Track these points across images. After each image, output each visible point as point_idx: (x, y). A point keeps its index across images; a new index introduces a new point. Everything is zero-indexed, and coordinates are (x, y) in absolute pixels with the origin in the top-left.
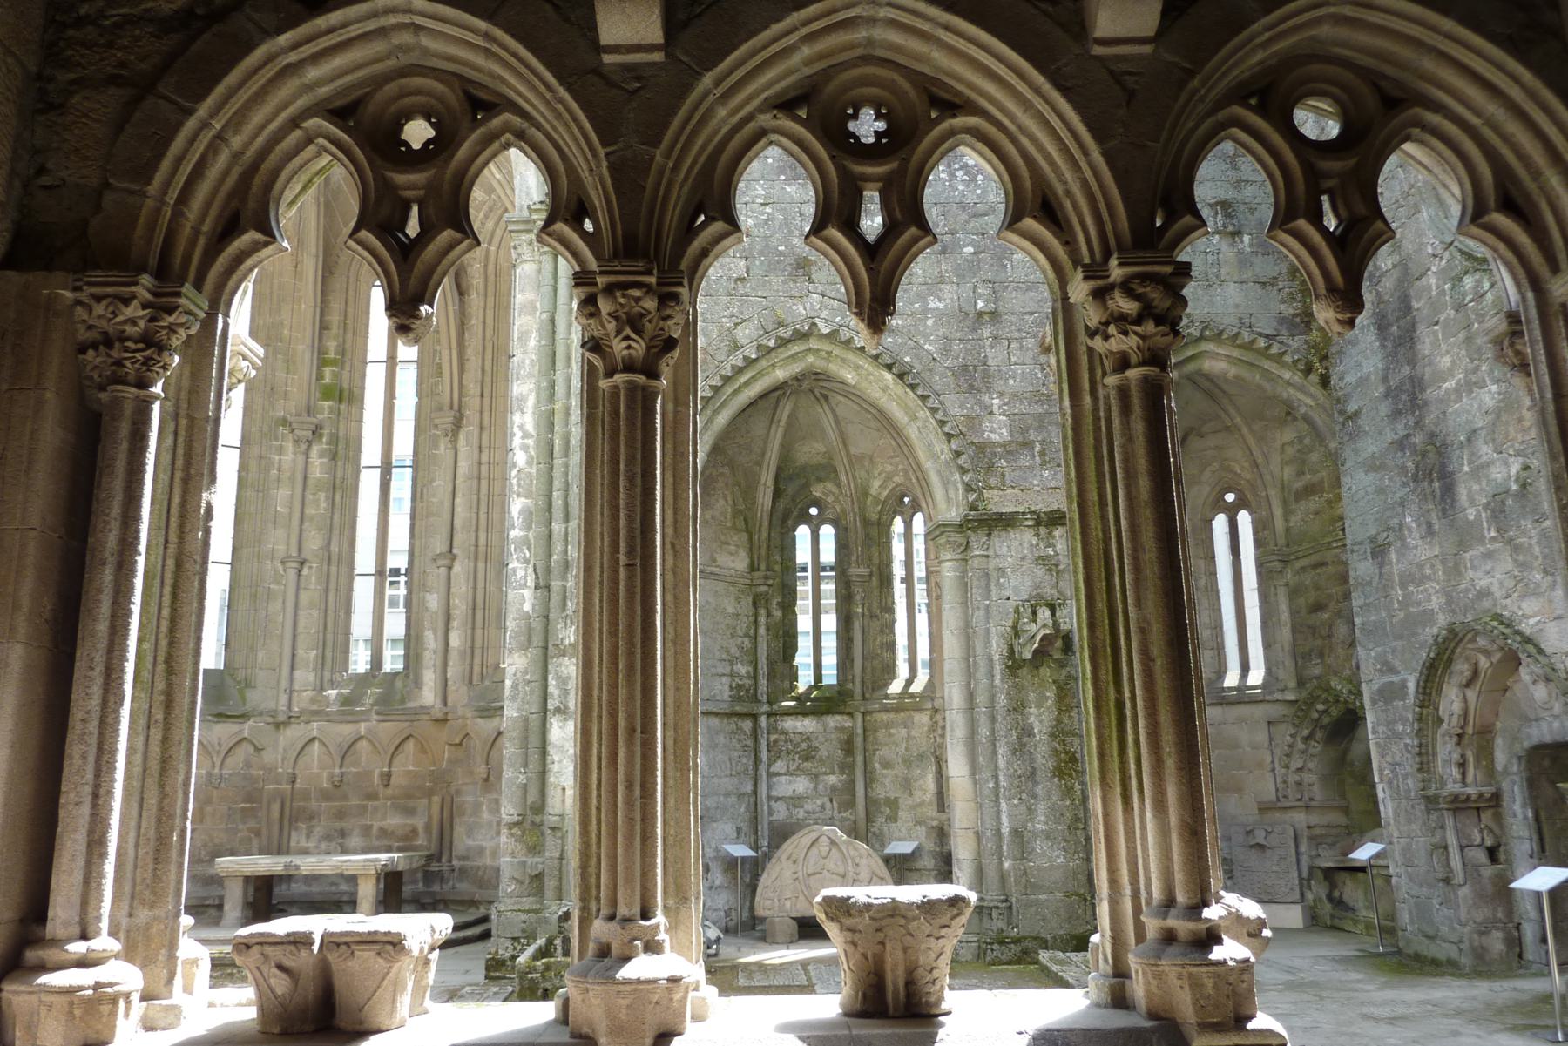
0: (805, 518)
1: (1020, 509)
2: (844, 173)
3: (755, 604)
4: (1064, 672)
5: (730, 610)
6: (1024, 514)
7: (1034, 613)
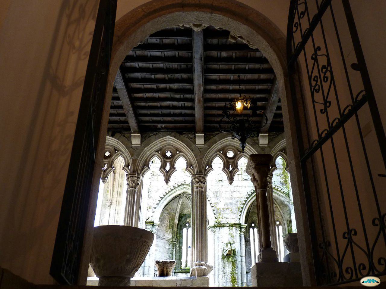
0: (185, 226)
1: (226, 223)
2: (164, 161)
3: (173, 246)
4: (234, 259)
5: (167, 247)
6: (227, 224)
7: (227, 245)
